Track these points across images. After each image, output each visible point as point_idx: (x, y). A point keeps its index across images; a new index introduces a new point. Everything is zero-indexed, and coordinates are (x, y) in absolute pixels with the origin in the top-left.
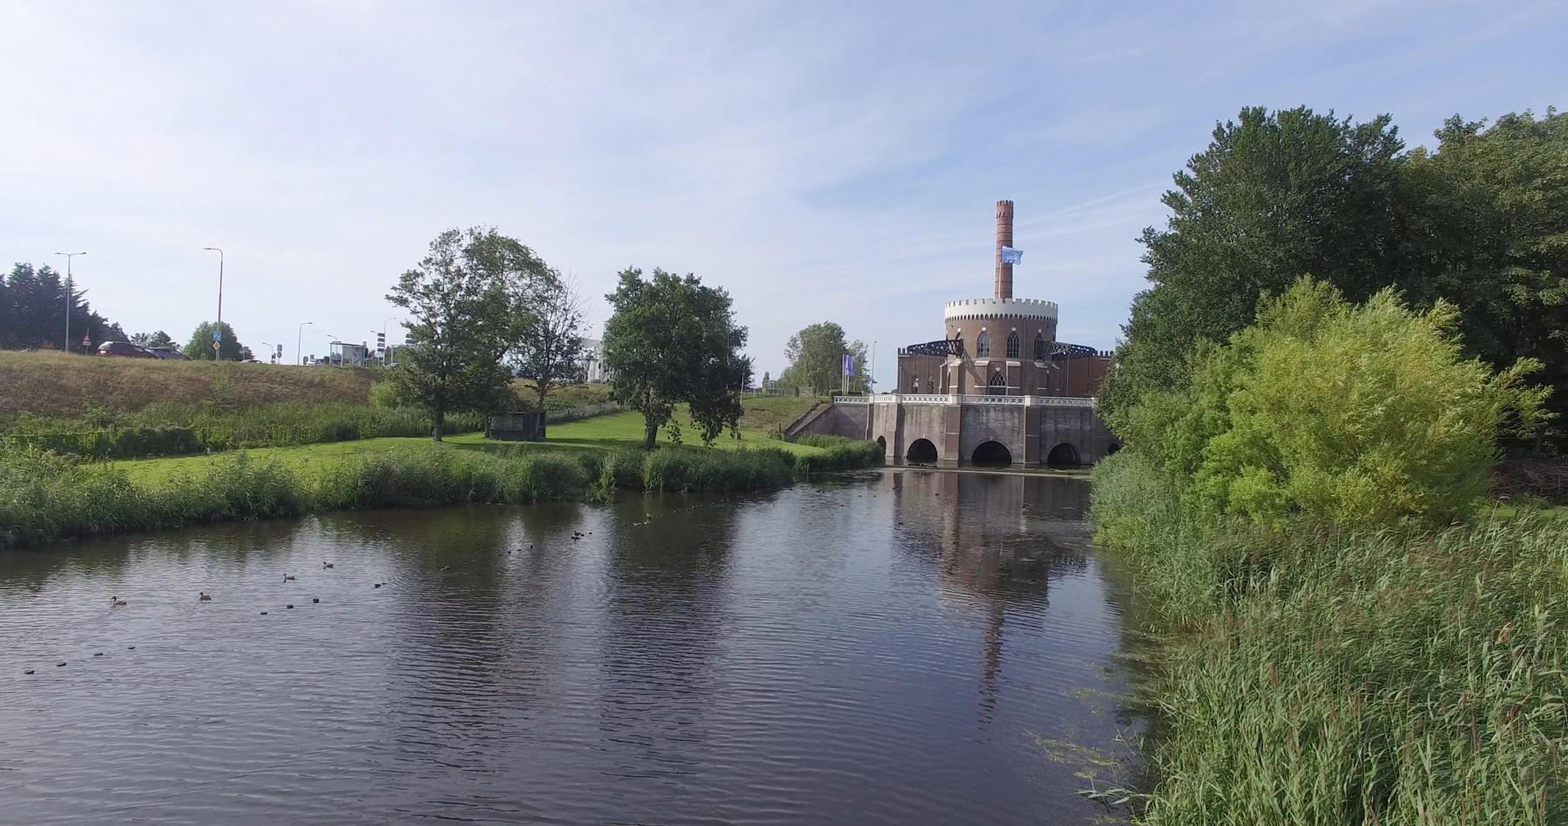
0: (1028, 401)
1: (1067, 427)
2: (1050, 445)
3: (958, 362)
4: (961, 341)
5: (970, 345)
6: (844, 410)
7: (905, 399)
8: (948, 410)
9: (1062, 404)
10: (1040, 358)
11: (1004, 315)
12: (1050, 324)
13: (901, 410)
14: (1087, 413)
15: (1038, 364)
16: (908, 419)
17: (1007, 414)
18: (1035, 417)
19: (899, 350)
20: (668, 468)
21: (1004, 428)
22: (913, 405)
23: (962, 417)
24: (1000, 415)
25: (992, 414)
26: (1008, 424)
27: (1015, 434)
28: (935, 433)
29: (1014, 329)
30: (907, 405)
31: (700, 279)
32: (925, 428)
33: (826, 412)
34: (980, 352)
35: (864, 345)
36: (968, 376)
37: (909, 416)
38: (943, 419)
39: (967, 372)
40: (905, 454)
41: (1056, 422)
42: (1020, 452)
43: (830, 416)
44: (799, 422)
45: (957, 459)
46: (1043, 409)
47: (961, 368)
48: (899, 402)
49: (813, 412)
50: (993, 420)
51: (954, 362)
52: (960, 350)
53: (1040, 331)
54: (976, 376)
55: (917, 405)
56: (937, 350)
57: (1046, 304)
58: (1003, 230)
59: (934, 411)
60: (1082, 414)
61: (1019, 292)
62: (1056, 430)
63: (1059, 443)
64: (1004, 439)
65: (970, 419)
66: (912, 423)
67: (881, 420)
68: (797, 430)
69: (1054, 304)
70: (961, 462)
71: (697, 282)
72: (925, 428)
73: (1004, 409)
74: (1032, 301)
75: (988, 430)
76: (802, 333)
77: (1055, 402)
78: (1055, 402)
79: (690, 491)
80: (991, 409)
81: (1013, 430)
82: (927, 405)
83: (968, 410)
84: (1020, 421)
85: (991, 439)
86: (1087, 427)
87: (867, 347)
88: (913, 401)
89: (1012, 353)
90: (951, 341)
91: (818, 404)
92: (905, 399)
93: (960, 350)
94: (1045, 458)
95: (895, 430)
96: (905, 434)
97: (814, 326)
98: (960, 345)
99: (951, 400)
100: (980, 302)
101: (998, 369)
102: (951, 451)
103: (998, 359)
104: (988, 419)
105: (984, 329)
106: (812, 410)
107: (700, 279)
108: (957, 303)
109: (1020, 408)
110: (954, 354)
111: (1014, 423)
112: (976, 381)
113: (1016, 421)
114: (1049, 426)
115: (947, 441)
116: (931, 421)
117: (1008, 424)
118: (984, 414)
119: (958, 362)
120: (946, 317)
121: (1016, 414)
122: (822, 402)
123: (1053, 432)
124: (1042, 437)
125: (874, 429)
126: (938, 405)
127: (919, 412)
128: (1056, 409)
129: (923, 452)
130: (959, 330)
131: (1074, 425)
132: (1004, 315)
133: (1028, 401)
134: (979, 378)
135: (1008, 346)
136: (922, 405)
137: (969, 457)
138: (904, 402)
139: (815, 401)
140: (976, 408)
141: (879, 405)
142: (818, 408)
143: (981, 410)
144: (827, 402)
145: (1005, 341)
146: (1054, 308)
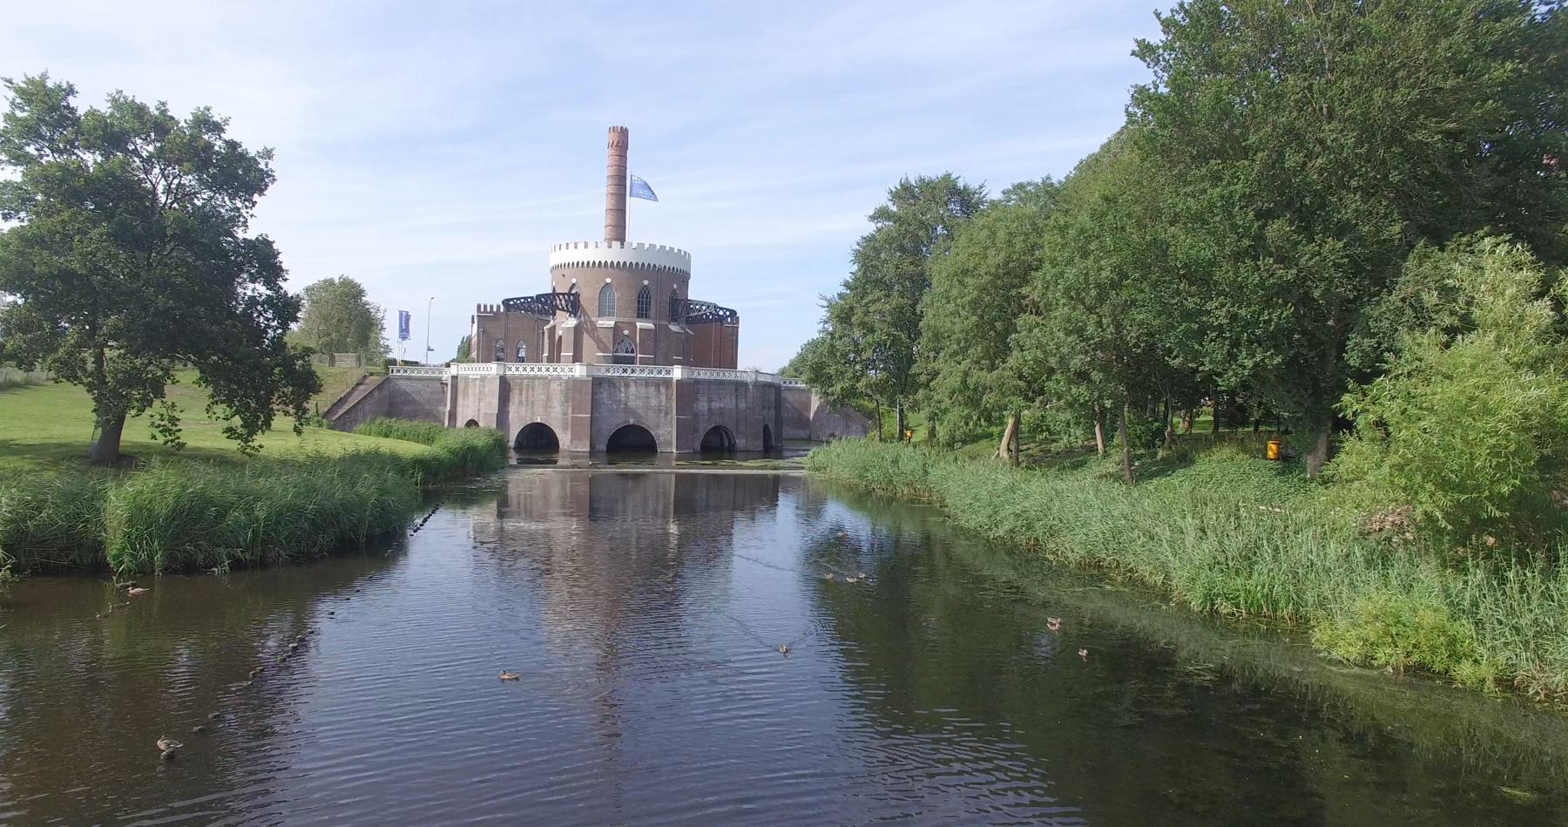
0: (677, 373)
1: (722, 405)
2: (703, 428)
3: (572, 322)
4: (577, 295)
6: (403, 385)
7: (510, 369)
8: (574, 384)
9: (715, 377)
10: (674, 318)
11: (634, 263)
12: (683, 278)
13: (505, 386)
14: (743, 389)
15: (674, 328)
16: (515, 398)
17: (652, 389)
18: (687, 391)
19: (479, 306)
20: (175, 514)
21: (647, 407)
22: (521, 378)
23: (594, 394)
24: (643, 390)
25: (632, 389)
26: (653, 402)
27: (663, 415)
28: (555, 416)
29: (646, 282)
30: (515, 377)
31: (226, 121)
32: (539, 409)
33: (379, 387)
35: (382, 309)
36: (586, 338)
37: (517, 392)
38: (566, 396)
39: (585, 334)
40: (512, 444)
41: (710, 400)
42: (669, 437)
43: (385, 393)
44: (342, 401)
45: (588, 450)
46: (697, 382)
47: (578, 330)
48: (501, 373)
49: (361, 387)
50: (634, 398)
51: (565, 323)
52: (574, 306)
53: (675, 286)
54: (598, 341)
55: (528, 377)
56: (544, 305)
57: (683, 253)
58: (616, 163)
59: (555, 386)
60: (736, 390)
61: (632, 237)
62: (710, 410)
63: (713, 425)
64: (649, 422)
66: (520, 402)
67: (471, 399)
69: (685, 253)
70: (593, 453)
71: (217, 128)
72: (539, 409)
73: (647, 383)
74: (668, 249)
75: (627, 410)
76: (307, 290)
77: (704, 374)
78: (704, 374)
79: (237, 565)
80: (632, 384)
82: (544, 378)
83: (601, 383)
84: (669, 399)
85: (632, 422)
86: (742, 405)
87: (385, 311)
88: (521, 372)
89: (642, 314)
90: (558, 295)
91: (365, 377)
92: (510, 369)
93: (574, 306)
94: (698, 446)
95: (497, 412)
96: (510, 417)
97: (325, 281)
98: (575, 299)
99: (579, 371)
100: (591, 246)
101: (626, 332)
102: (580, 439)
103: (627, 320)
104: (627, 397)
105: (608, 280)
106: (358, 384)
107: (226, 121)
108: (564, 247)
110: (568, 311)
111: (660, 401)
112: (598, 347)
113: (663, 398)
114: (702, 405)
115: (575, 425)
116: (548, 398)
117: (653, 402)
118: (623, 390)
119: (572, 322)
120: (551, 265)
121: (663, 389)
122: (372, 374)
123: (706, 413)
124: (696, 415)
125: (459, 409)
126: (559, 378)
127: (531, 387)
128: (709, 382)
129: (539, 442)
130: (574, 281)
131: (728, 403)
132: (634, 263)
133: (677, 373)
134: (602, 342)
135: (638, 304)
136: (535, 378)
137: (602, 446)
138: (508, 373)
139: (361, 372)
140: (610, 382)
141: (466, 378)
142: (367, 381)
143: (618, 384)
144: (378, 374)
145: (635, 297)
146: (685, 257)
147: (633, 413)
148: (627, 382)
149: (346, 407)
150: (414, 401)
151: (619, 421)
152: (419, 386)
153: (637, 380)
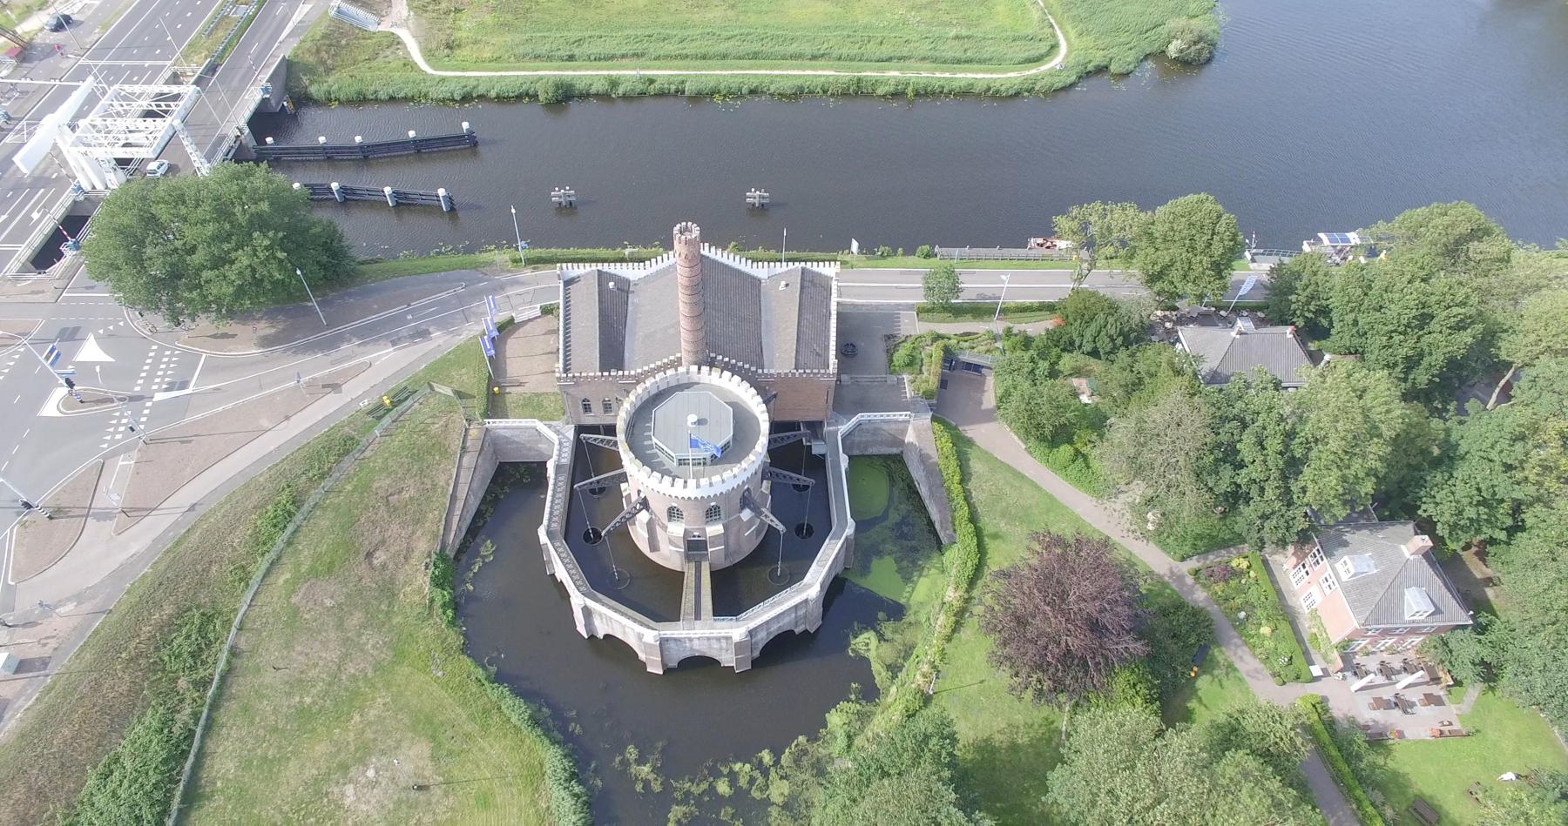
0: (736, 630)
5: (659, 507)
6: (502, 432)
15: (746, 514)
22: (600, 615)
34: (673, 513)
39: (657, 527)
44: (453, 498)
49: (466, 460)
65: (672, 645)
68: (454, 527)
81: (721, 649)
86: (801, 612)
89: (712, 513)
94: (756, 654)
109: (728, 638)
121: (723, 641)
128: (767, 622)
147: (697, 651)
148: (691, 640)
149: (458, 512)
150: (514, 442)
151: (688, 654)
152: (517, 432)
153: (699, 639)
